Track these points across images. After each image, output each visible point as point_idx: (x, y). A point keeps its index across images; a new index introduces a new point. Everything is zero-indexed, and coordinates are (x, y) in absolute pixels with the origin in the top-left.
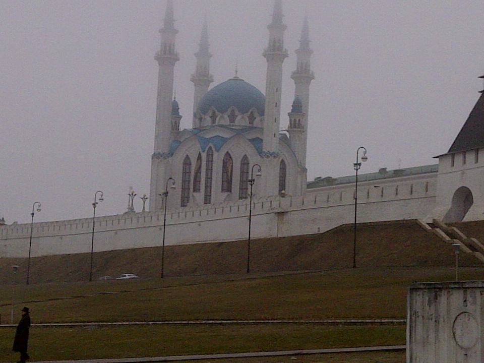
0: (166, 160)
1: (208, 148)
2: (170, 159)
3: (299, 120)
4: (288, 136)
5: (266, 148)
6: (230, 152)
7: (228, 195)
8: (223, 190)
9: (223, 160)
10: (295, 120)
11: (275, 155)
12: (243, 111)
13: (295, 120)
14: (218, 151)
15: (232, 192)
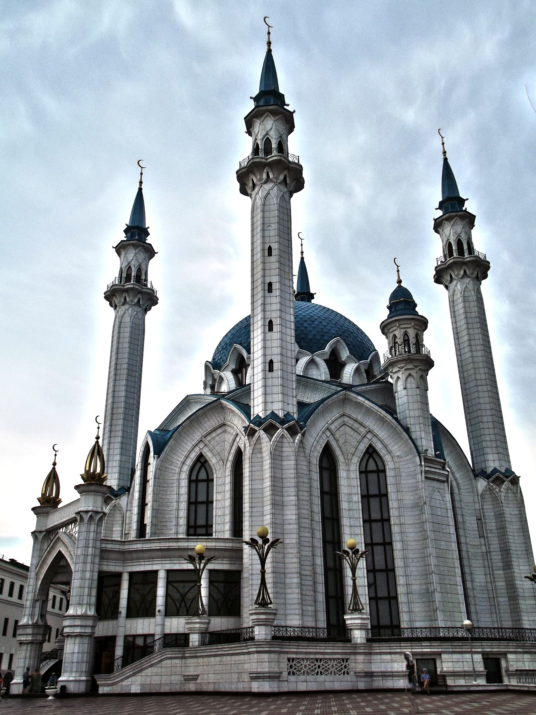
3: (406, 334)
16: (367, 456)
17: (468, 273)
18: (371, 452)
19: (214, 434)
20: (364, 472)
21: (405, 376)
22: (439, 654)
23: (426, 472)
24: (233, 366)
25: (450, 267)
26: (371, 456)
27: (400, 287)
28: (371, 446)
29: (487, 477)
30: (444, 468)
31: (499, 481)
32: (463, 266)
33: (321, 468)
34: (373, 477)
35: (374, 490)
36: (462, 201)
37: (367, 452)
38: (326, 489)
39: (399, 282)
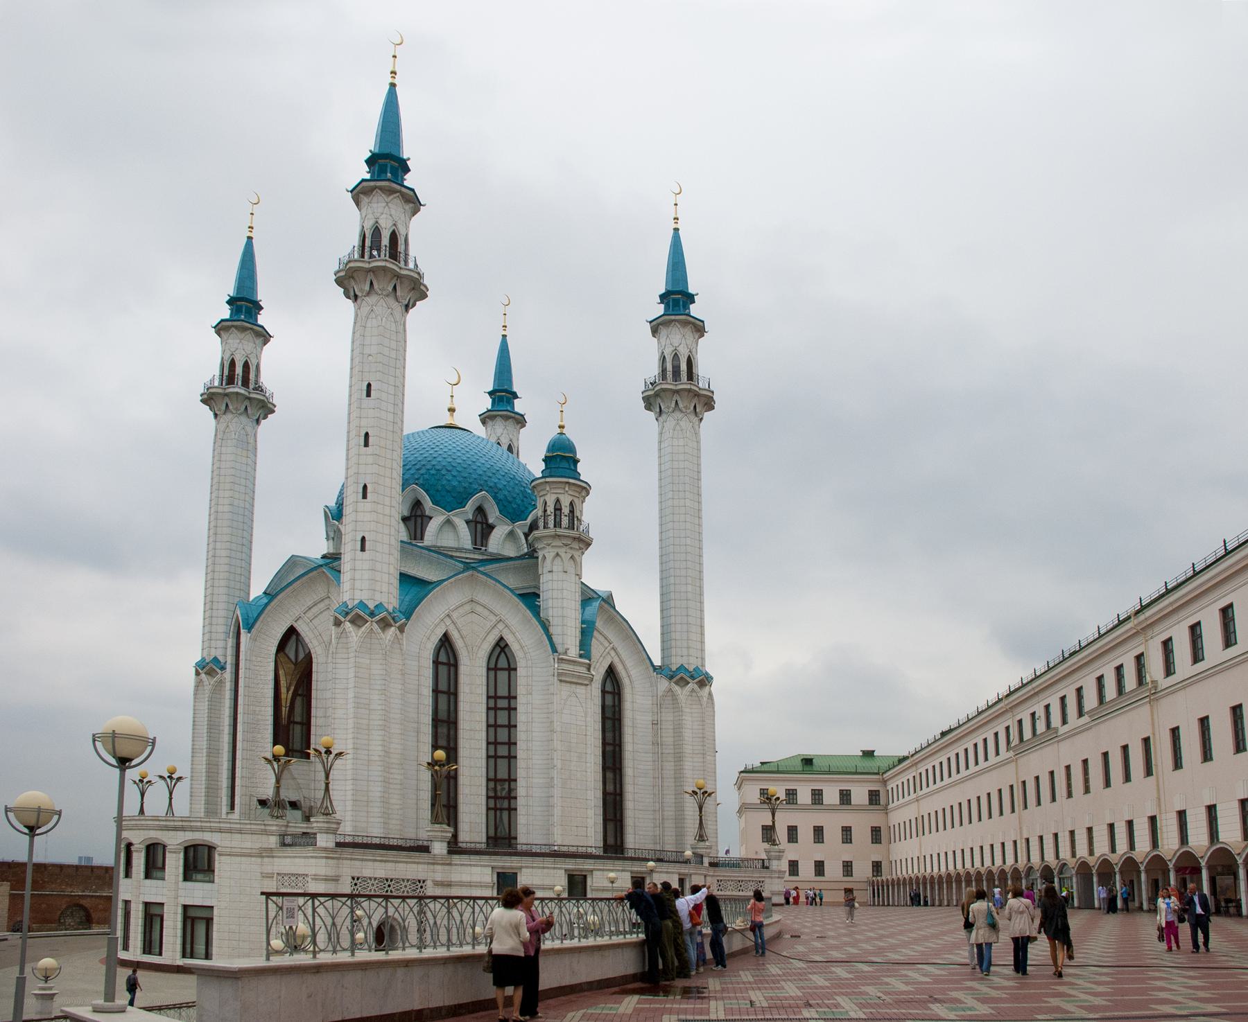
6: (301, 628)
14: (249, 629)
16: (498, 650)
17: (681, 405)
18: (501, 647)
20: (493, 669)
21: (553, 554)
22: (521, 868)
23: (559, 674)
25: (657, 395)
26: (503, 650)
28: (501, 639)
30: (589, 670)
32: (678, 392)
33: (436, 663)
34: (503, 676)
36: (690, 298)
37: (497, 644)
38: (443, 686)
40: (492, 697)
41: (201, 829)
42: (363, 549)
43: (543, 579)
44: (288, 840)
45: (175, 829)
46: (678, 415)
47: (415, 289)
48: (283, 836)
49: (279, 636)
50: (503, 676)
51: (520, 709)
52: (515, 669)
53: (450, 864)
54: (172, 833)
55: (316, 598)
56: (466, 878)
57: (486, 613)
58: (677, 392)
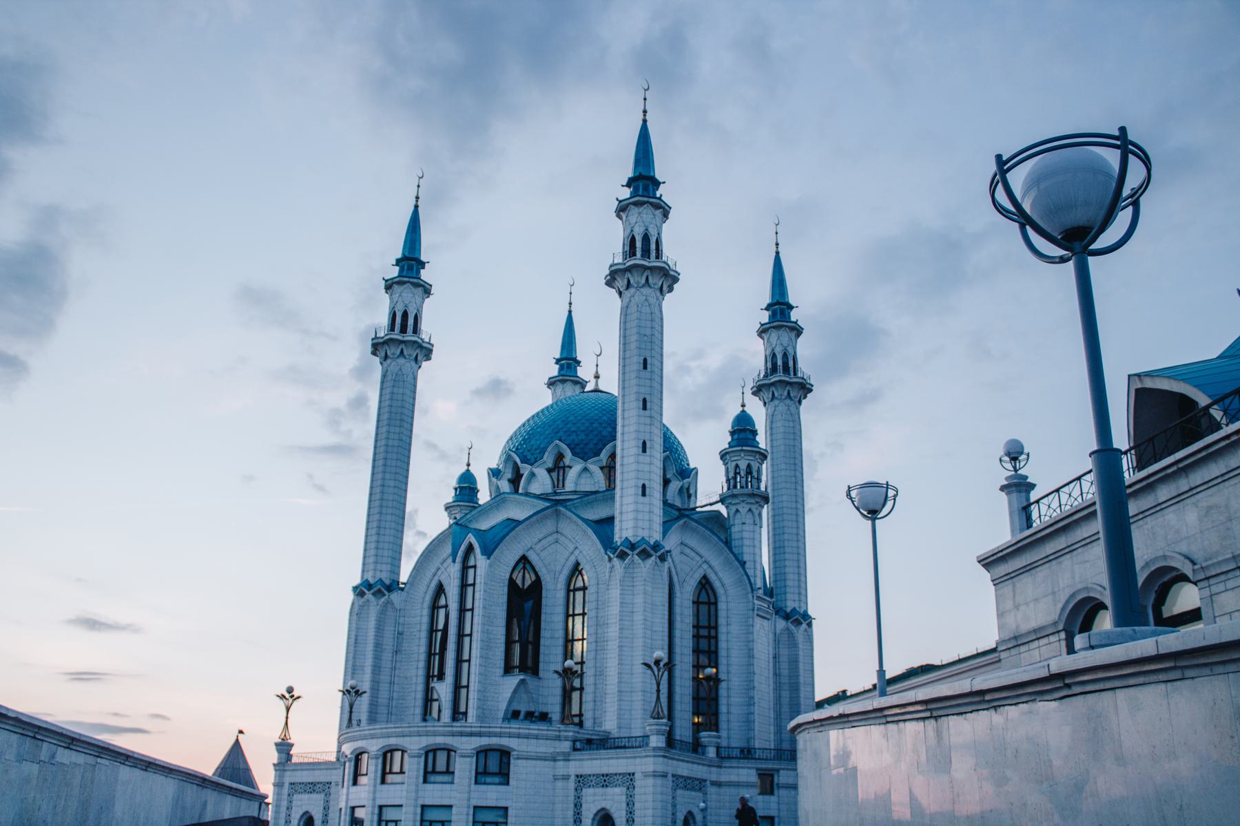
0: (383, 600)
1: (463, 548)
2: (395, 597)
3: (749, 466)
4: (724, 511)
5: (624, 531)
6: (532, 557)
7: (522, 681)
8: (508, 670)
9: (512, 582)
10: (737, 466)
11: (646, 550)
12: (585, 452)
13: (737, 466)
14: (488, 552)
15: (541, 674)
18: (705, 584)
19: (544, 542)
20: (697, 603)
24: (550, 465)
27: (743, 411)
28: (705, 577)
29: (787, 617)
31: (798, 623)
35: (704, 622)
39: (743, 406)
40: (697, 627)
41: (500, 735)
42: (644, 494)
43: (735, 529)
44: (578, 745)
45: (471, 734)
46: (788, 401)
47: (669, 278)
48: (574, 741)
49: (513, 563)
50: (704, 609)
51: (722, 637)
52: (716, 604)
53: (720, 767)
54: (464, 739)
55: (545, 531)
56: (734, 778)
57: (693, 554)
58: (790, 384)
